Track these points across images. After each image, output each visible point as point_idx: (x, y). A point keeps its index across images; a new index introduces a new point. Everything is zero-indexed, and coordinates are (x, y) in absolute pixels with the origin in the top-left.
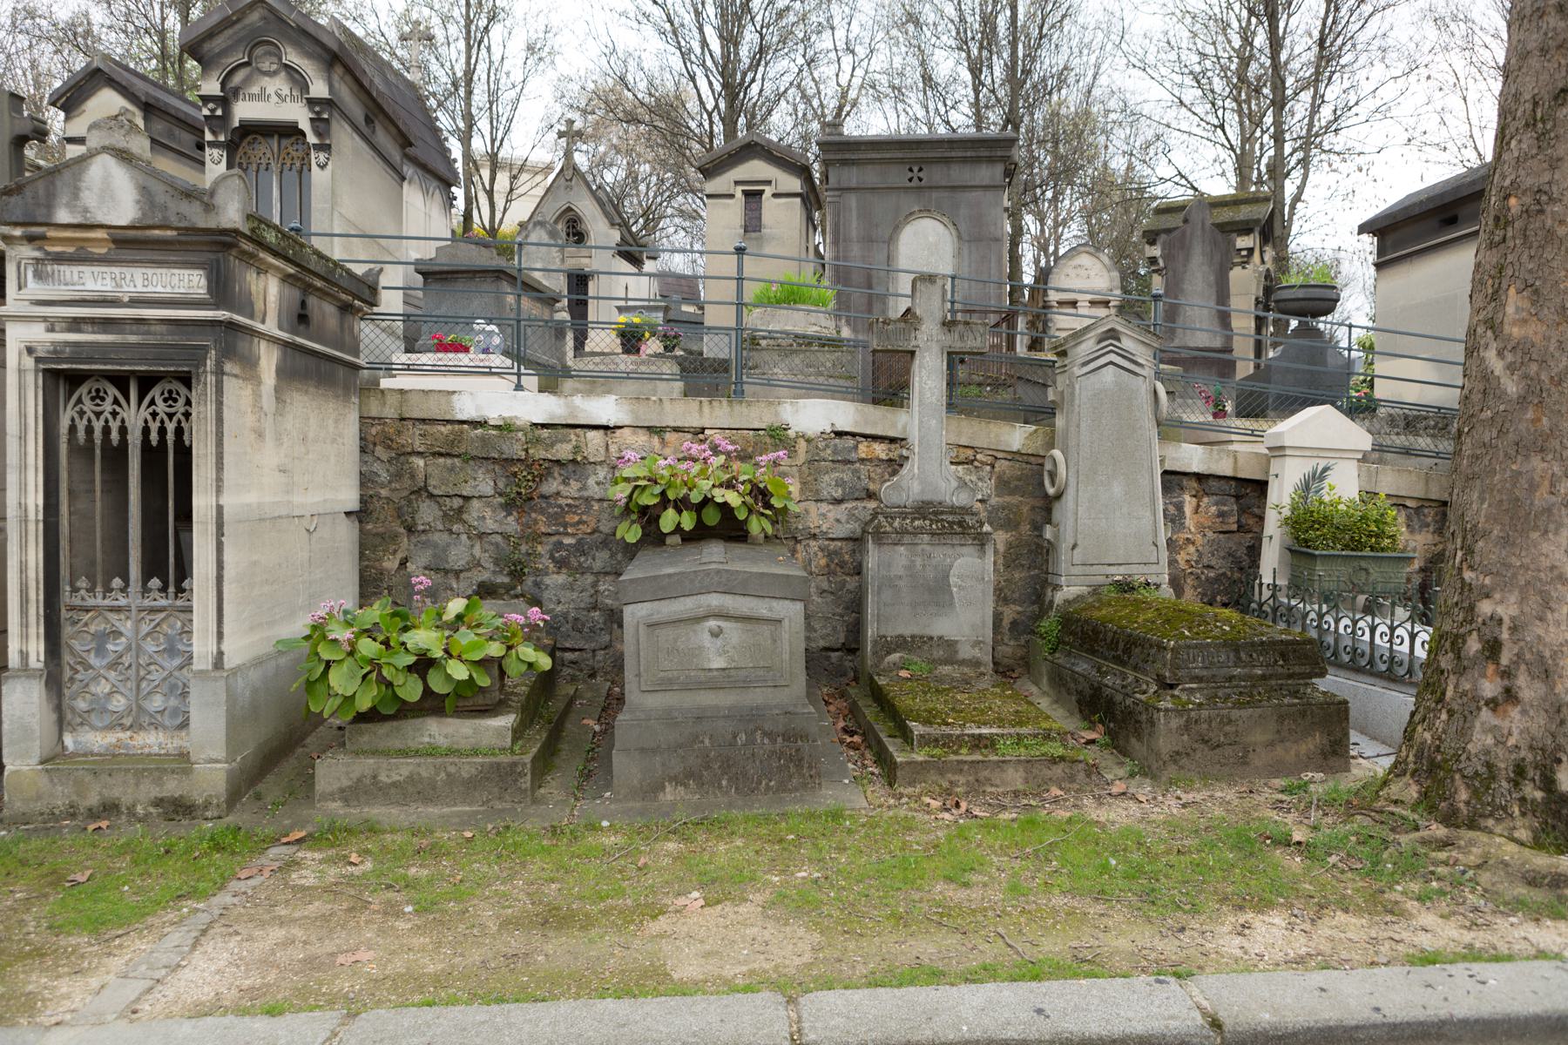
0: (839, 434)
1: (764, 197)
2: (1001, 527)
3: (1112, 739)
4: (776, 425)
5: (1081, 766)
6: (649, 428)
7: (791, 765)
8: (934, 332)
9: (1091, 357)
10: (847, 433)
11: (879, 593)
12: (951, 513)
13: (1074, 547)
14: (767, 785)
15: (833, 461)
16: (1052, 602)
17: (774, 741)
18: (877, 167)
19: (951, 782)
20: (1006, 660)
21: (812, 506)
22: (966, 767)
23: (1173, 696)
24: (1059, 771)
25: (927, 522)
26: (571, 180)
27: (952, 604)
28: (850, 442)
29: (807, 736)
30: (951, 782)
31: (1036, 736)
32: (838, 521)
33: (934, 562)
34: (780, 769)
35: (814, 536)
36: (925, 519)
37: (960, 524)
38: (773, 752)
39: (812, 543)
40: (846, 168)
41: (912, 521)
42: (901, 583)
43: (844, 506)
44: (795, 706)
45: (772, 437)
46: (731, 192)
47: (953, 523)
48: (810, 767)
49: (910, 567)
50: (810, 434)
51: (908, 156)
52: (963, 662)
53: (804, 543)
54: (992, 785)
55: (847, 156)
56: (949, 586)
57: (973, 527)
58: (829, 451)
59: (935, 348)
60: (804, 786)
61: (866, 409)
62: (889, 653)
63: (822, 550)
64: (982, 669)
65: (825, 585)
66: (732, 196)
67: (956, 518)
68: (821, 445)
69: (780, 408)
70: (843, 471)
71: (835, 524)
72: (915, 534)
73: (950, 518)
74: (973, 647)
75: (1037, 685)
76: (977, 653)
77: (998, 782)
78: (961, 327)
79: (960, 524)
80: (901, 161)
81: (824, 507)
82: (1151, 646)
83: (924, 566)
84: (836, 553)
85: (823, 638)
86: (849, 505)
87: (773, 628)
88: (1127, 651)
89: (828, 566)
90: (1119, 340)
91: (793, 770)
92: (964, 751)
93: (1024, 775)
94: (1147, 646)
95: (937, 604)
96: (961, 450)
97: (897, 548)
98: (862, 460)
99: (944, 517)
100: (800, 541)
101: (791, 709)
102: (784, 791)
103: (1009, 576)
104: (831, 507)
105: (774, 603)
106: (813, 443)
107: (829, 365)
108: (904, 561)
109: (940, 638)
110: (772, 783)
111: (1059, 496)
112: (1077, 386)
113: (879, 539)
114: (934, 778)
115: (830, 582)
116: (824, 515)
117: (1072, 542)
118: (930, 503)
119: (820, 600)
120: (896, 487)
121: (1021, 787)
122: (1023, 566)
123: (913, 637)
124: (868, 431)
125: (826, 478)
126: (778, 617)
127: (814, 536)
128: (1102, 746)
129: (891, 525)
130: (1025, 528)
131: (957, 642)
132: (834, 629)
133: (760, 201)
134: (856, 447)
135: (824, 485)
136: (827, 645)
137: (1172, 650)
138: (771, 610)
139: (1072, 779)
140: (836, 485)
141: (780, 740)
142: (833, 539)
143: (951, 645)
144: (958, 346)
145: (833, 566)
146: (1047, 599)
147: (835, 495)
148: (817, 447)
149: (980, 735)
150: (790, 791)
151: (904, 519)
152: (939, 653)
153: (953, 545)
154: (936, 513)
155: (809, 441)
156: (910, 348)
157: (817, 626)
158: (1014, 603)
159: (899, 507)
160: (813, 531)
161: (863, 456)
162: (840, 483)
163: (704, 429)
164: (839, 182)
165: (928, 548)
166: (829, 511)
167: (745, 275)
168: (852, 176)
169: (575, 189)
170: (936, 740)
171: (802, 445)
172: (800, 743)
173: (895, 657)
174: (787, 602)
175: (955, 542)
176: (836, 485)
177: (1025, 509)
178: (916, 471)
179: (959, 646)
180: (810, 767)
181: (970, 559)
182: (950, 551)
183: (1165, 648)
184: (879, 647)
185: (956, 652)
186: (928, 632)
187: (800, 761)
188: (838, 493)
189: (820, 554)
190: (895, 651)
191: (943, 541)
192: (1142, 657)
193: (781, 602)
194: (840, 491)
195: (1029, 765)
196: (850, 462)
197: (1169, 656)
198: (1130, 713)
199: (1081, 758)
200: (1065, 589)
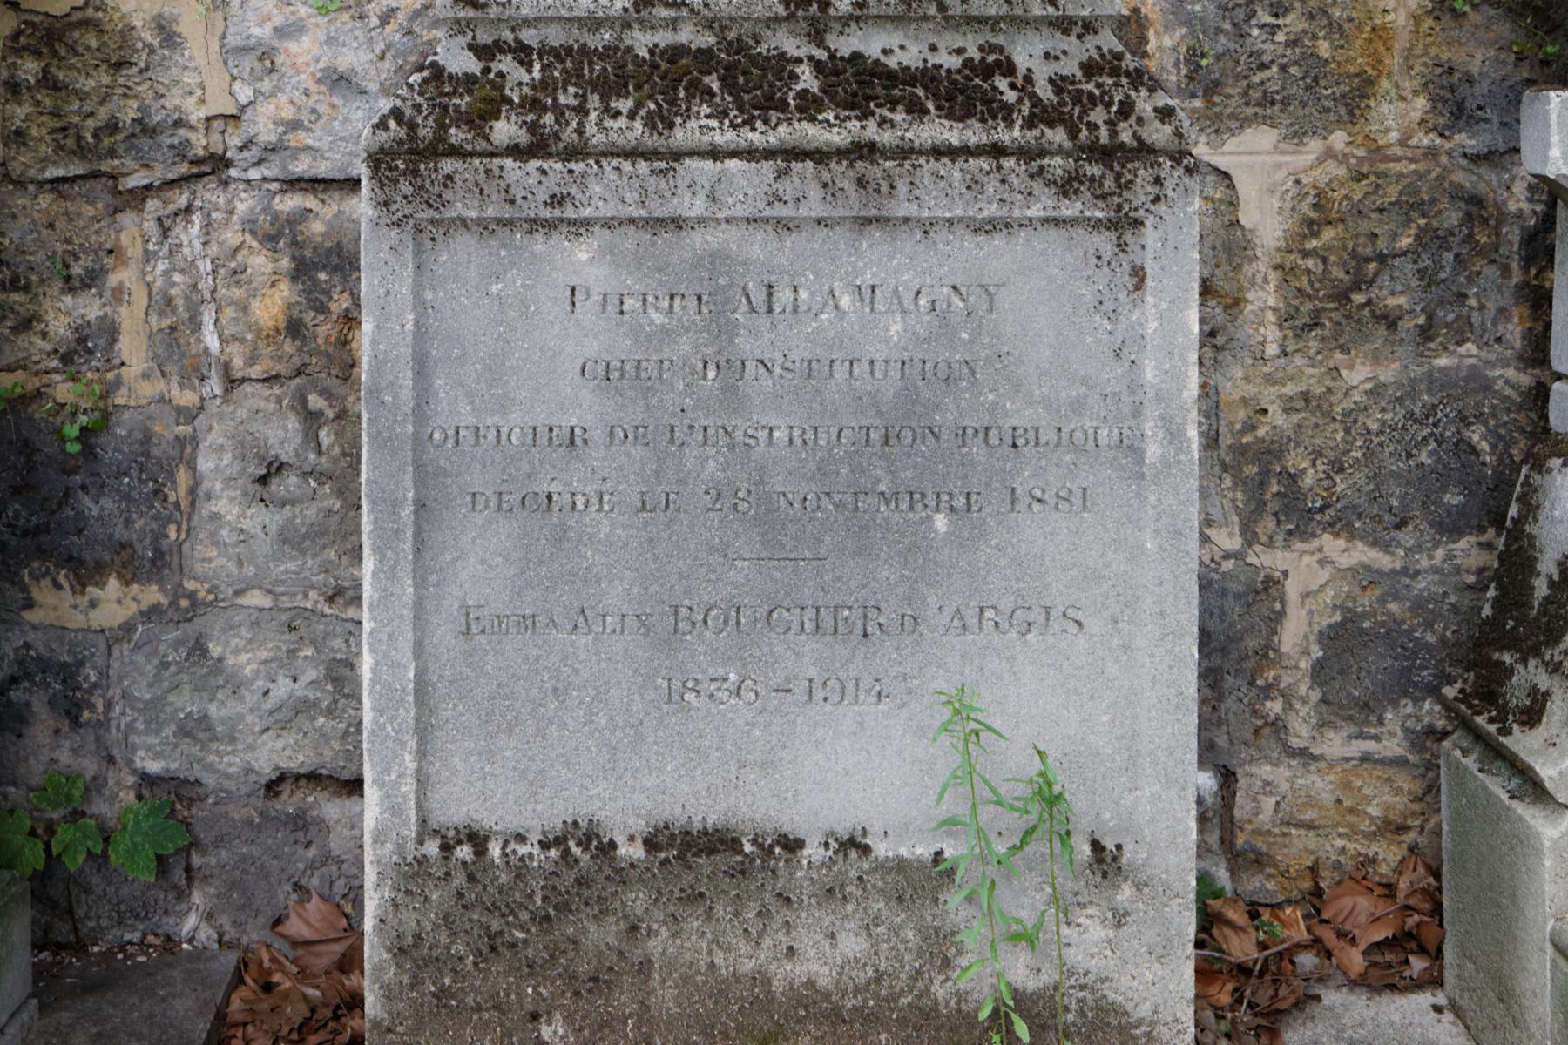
2: (1265, 108)
32: (339, 81)
71: (322, 99)
89: (294, 328)
95: (828, 624)
119: (258, 520)
122: (1390, 321)
136: (299, 760)
158: (1341, 525)
175: (934, 205)
189: (260, 262)
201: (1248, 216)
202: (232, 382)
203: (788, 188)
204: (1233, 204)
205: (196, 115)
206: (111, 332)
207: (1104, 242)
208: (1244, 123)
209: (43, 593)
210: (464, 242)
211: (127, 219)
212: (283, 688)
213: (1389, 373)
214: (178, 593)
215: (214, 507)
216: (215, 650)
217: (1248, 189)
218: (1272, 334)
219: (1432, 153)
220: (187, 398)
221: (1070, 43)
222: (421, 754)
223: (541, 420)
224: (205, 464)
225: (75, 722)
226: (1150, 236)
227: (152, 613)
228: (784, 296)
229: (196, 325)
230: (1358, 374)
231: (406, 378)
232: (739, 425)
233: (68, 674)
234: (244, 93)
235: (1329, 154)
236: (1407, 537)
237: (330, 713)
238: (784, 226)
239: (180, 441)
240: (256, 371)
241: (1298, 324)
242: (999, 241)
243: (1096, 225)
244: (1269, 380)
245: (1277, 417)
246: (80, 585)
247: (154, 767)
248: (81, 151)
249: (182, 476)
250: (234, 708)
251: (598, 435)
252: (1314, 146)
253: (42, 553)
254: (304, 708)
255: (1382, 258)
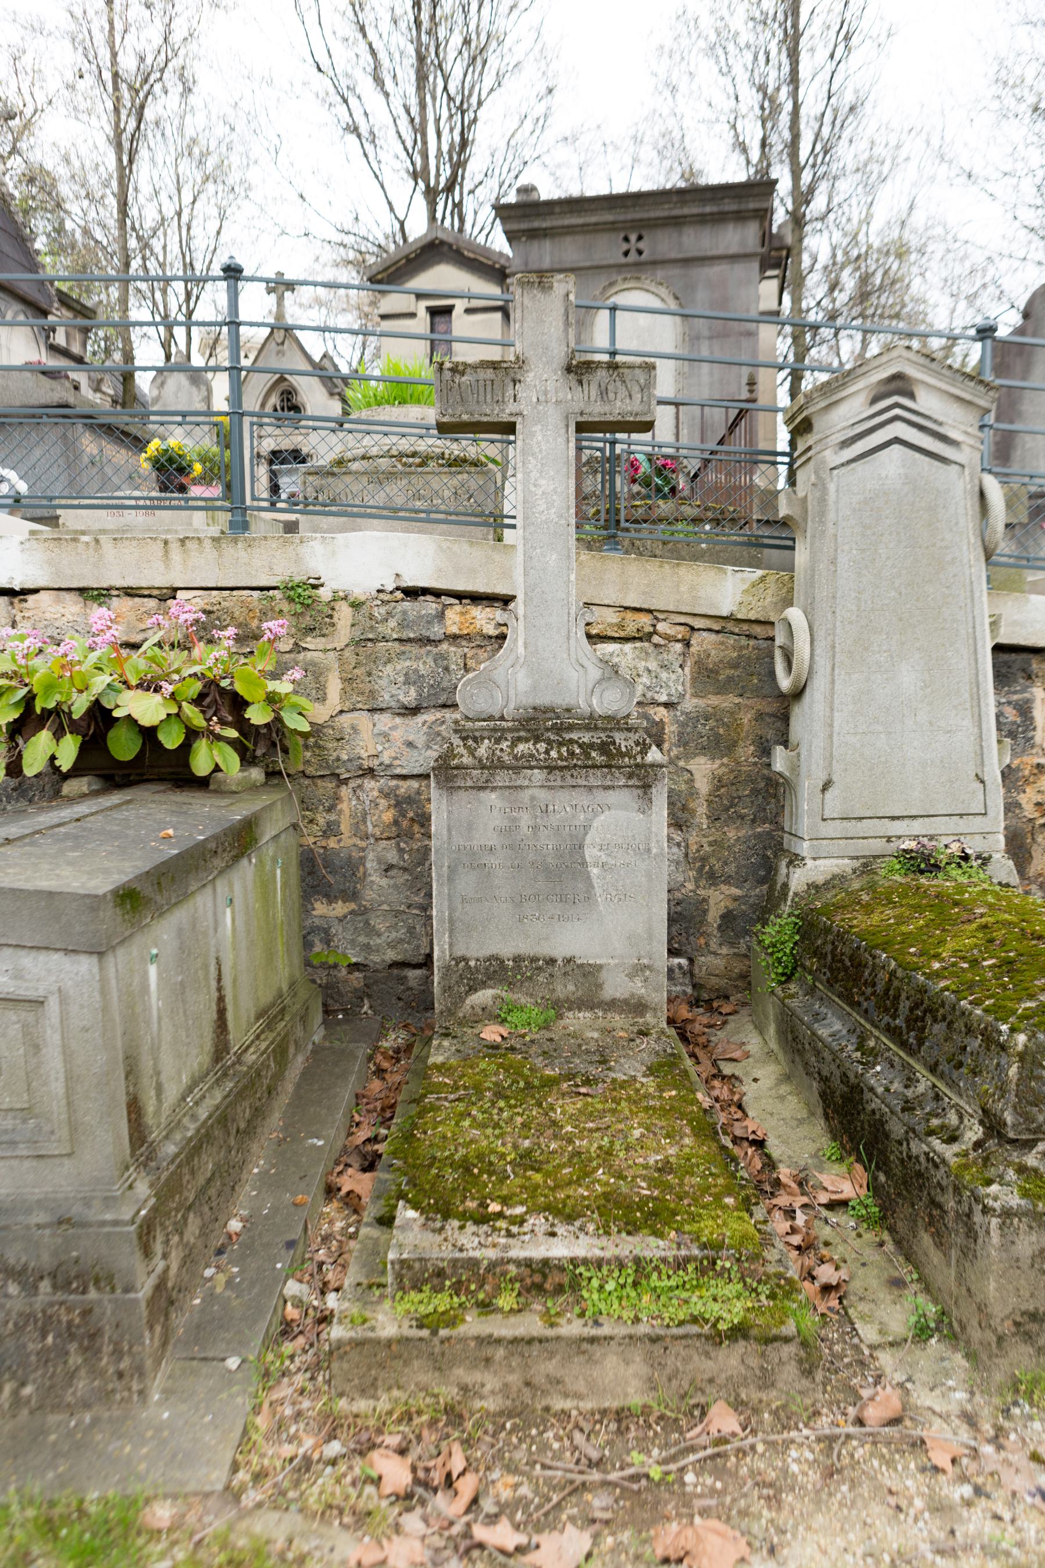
0: (412, 593)
1: (454, 313)
2: (703, 750)
3: (883, 1208)
4: (297, 579)
5: (789, 1350)
6: (81, 591)
7: (73, 1347)
8: (551, 386)
9: (851, 433)
10: (425, 591)
11: (451, 879)
12: (587, 728)
13: (826, 786)
14: (15, 1393)
15: (400, 640)
16: (786, 886)
17: (32, 1289)
18: (580, 239)
19: (465, 1389)
20: (714, 980)
21: (362, 719)
22: (501, 1352)
23: (1021, 1169)
24: (734, 1361)
25: (542, 746)
26: (283, 343)
27: (589, 897)
28: (429, 606)
29: (110, 1278)
30: (465, 1389)
31: (680, 1264)
32: (410, 744)
33: (554, 820)
34: (45, 1357)
35: (370, 772)
36: (537, 739)
37: (604, 748)
38: (28, 1317)
39: (369, 784)
40: (535, 244)
41: (513, 745)
42: (492, 860)
43: (420, 718)
44: (87, 1202)
45: (291, 600)
46: (412, 309)
47: (592, 746)
48: (118, 1354)
49: (510, 830)
50: (359, 593)
51: (622, 218)
52: (612, 1005)
53: (352, 784)
54: (566, 1395)
55: (536, 224)
56: (584, 863)
57: (628, 754)
58: (392, 623)
59: (554, 417)
60: (106, 1396)
61: (456, 547)
62: (472, 989)
63: (385, 794)
64: (649, 1018)
65: (392, 857)
66: (412, 315)
67: (601, 736)
68: (379, 612)
69: (304, 550)
70: (418, 658)
72: (517, 769)
73: (586, 738)
74: (631, 976)
75: (761, 1033)
76: (638, 988)
77: (581, 1386)
78: (602, 374)
79: (604, 748)
80: (611, 227)
81: (385, 721)
82: (969, 1031)
83: (535, 828)
84: (409, 800)
85: (391, 945)
86: (429, 717)
87: (31, 1018)
88: (915, 1022)
89: (396, 823)
90: (912, 396)
91: (75, 1359)
92: (506, 1301)
93: (644, 1370)
94: (959, 1025)
95: (562, 899)
96: (629, 615)
97: (482, 795)
98: (454, 638)
99: (574, 736)
100: (345, 781)
101: (76, 1210)
102: (56, 1408)
103: (717, 836)
104: (398, 720)
105: (28, 961)
106: (364, 610)
107: (447, 493)
108: (497, 820)
109: (569, 961)
110: (28, 1390)
111: (798, 694)
112: (832, 487)
113: (449, 779)
114: (424, 1378)
115: (401, 851)
116: (385, 735)
117: (821, 778)
118: (547, 710)
119: (384, 882)
120: (488, 682)
121: (636, 1399)
122: (742, 817)
123: (517, 959)
124: (460, 586)
125: (389, 668)
126: (32, 994)
127: (370, 772)
128: (861, 1219)
129: (472, 752)
130: (746, 752)
131: (600, 967)
132: (411, 930)
133: (450, 322)
134: (441, 616)
135: (383, 683)
136: (399, 958)
137: (1022, 1057)
138: (18, 975)
139: (766, 1380)
140: (407, 682)
141: (45, 1286)
142: (404, 777)
143: (590, 973)
144: (597, 411)
145: (405, 824)
146: (781, 879)
147: (405, 700)
148: (371, 617)
149: (546, 1262)
150: (71, 1410)
151: (498, 741)
152: (566, 989)
153: (590, 788)
154: (558, 729)
155: (356, 605)
156: (505, 418)
157: (381, 927)
158: (727, 881)
159: (491, 718)
160: (366, 764)
161: (454, 629)
162: (411, 679)
163: (176, 589)
164: (526, 264)
165: (542, 795)
166: (394, 728)
167: (242, 317)
168: (545, 253)
169: (288, 354)
170: (440, 1274)
171: (344, 614)
172: (93, 1294)
173: (484, 996)
174: (56, 957)
175: (593, 782)
176: (407, 682)
177: (746, 718)
178: (521, 650)
179: (604, 975)
180: (118, 1354)
181: (622, 814)
182: (581, 798)
183: (1003, 1048)
184: (455, 978)
185: (599, 986)
186: (546, 950)
187: (93, 1336)
188: (410, 697)
190: (484, 985)
191: (571, 781)
192: (949, 1048)
193: (43, 957)
194: (413, 692)
195: (658, 1350)
196: (430, 641)
197: (1013, 1071)
198: (919, 1175)
199: (789, 1328)
200: (810, 863)
201: (697, 785)
202: (377, 840)
203: (551, 777)
204: (693, 781)
205: (365, 755)
206: (338, 823)
207: (640, 792)
208: (696, 755)
209: (318, 905)
210: (462, 793)
211: (344, 788)
212: (394, 935)
213: (742, 833)
214: (360, 905)
215: (373, 878)
216: (372, 922)
217: (697, 776)
218: (705, 822)
219: (755, 764)
220: (363, 844)
221: (631, 735)
222: (450, 937)
223: (482, 843)
224: (368, 865)
225: (329, 946)
226: (654, 790)
227: (352, 912)
228: (551, 808)
229: (364, 821)
230: (732, 834)
231: (445, 832)
232: (538, 844)
233: (326, 931)
234: (380, 748)
235: (723, 764)
236: (747, 885)
237: (408, 943)
238: (550, 788)
239: (361, 858)
240: (385, 835)
241: (714, 819)
242: (611, 792)
243: (637, 787)
244: (704, 836)
245: (707, 848)
246: (330, 903)
247: (354, 960)
248: (328, 767)
249: (361, 869)
250: (379, 941)
251: (498, 847)
252: (718, 762)
253: (318, 893)
254: (401, 941)
255: (739, 797)
